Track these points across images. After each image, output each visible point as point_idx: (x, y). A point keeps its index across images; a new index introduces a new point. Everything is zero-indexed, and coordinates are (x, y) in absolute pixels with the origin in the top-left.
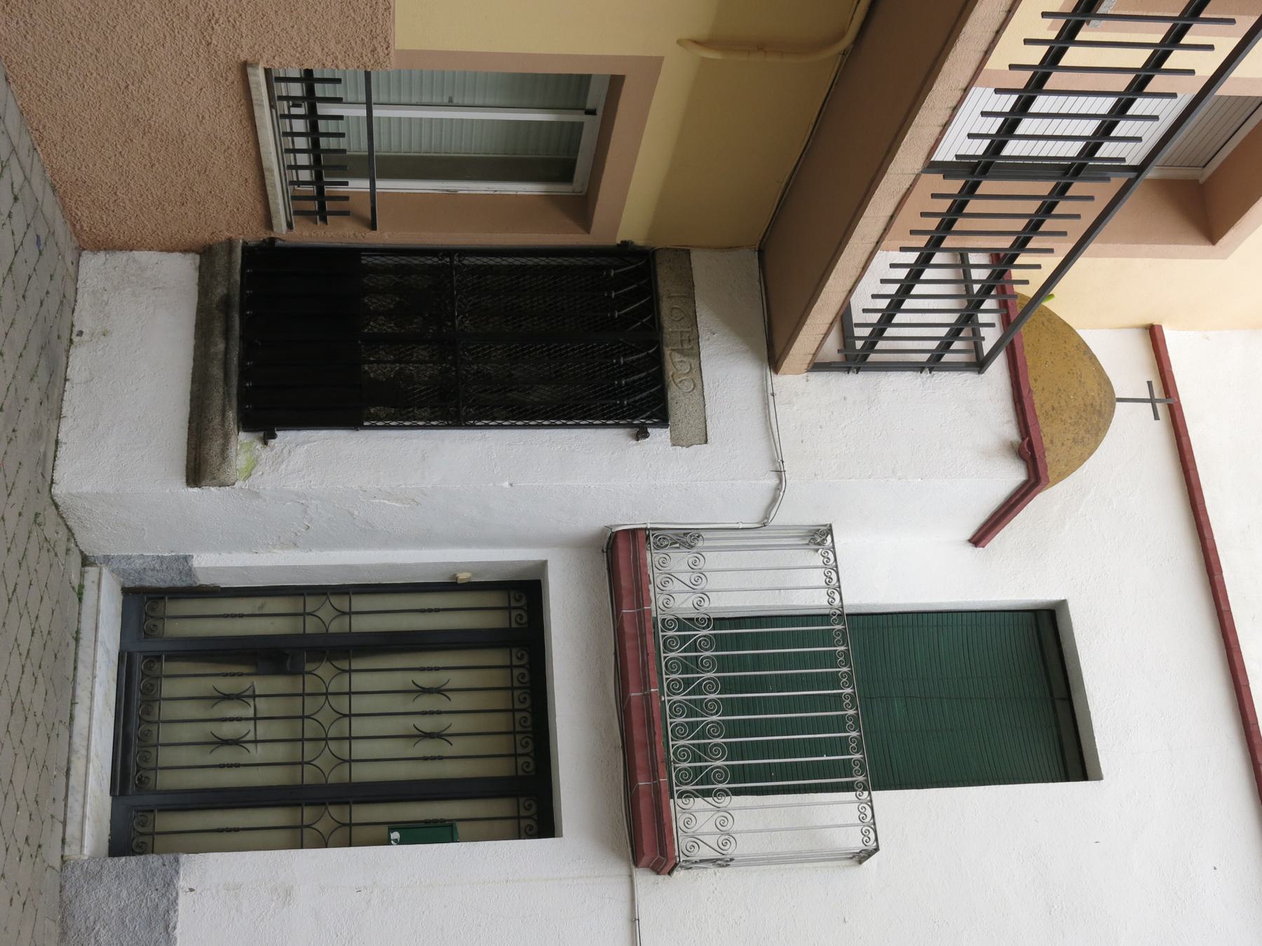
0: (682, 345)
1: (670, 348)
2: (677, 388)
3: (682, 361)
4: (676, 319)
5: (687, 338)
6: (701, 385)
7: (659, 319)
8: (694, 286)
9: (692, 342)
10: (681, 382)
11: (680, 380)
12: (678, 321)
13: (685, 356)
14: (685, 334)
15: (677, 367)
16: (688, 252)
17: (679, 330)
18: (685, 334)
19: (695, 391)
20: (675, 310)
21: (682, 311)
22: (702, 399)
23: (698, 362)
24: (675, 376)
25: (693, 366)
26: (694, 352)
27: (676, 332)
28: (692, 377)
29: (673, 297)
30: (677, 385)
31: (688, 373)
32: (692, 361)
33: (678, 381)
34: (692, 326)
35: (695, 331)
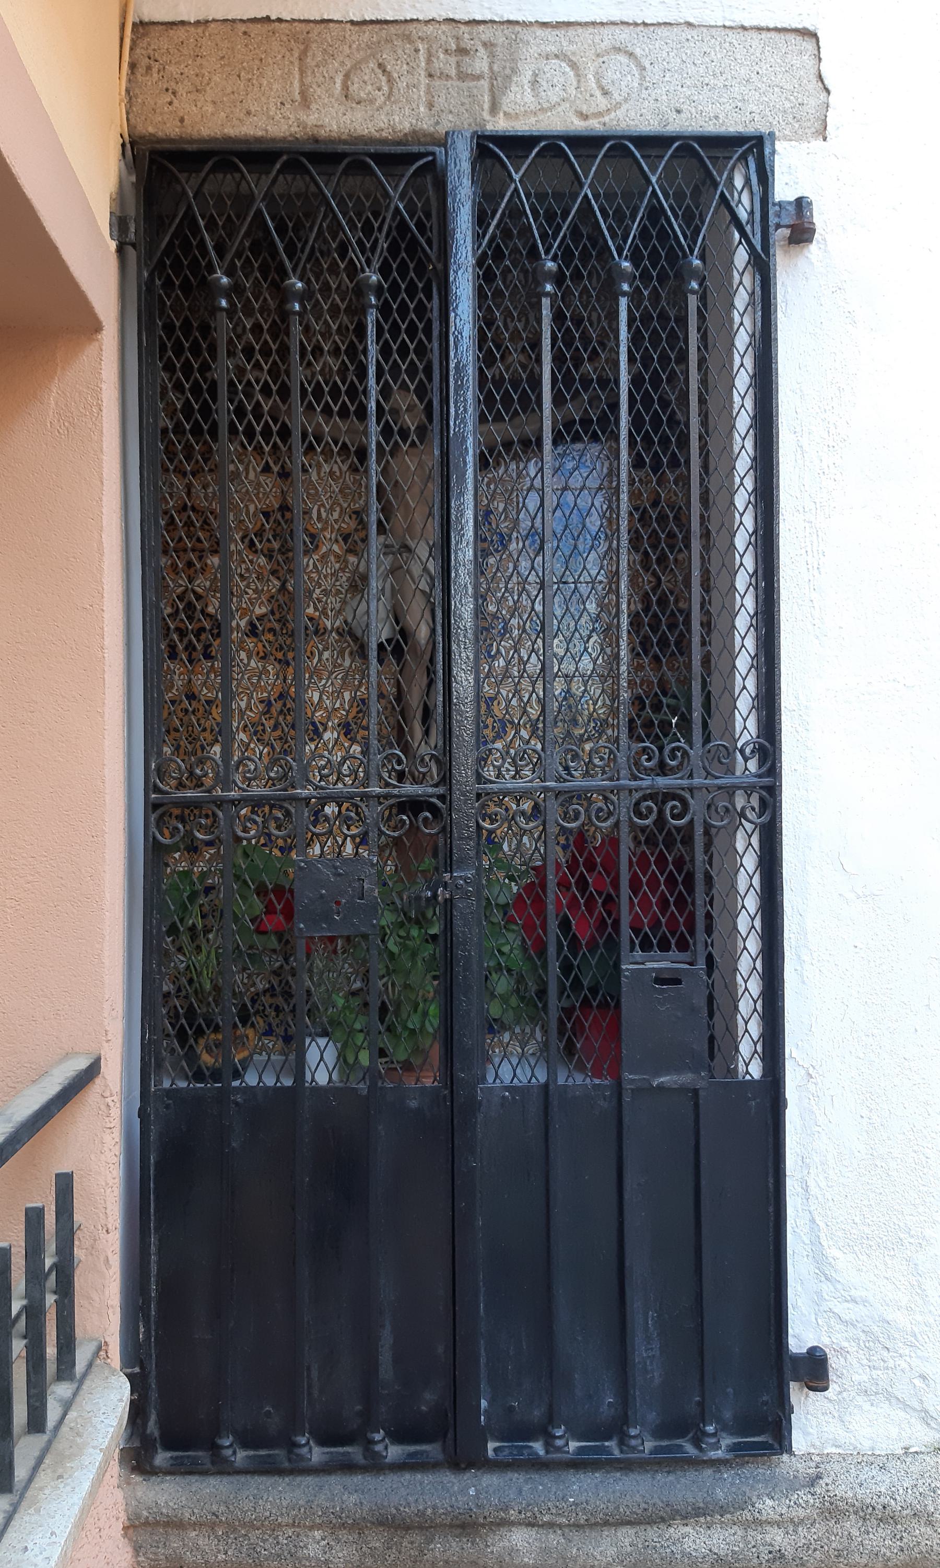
0: (479, 77)
1: (486, 115)
2: (625, 107)
3: (534, 83)
4: (386, 88)
5: (453, 60)
6: (617, 30)
7: (384, 142)
8: (267, 19)
9: (467, 43)
10: (605, 93)
11: (598, 93)
12: (390, 81)
13: (514, 71)
14: (437, 65)
15: (554, 99)
16: (142, 26)
17: (424, 80)
18: (437, 65)
19: (638, 52)
20: (354, 88)
21: (356, 66)
22: (663, 32)
23: (539, 32)
24: (584, 108)
25: (553, 49)
26: (501, 40)
27: (428, 92)
28: (591, 54)
29: (303, 93)
30: (618, 105)
31: (573, 65)
32: (533, 50)
33: (602, 103)
34: (411, 42)
35: (430, 29)
